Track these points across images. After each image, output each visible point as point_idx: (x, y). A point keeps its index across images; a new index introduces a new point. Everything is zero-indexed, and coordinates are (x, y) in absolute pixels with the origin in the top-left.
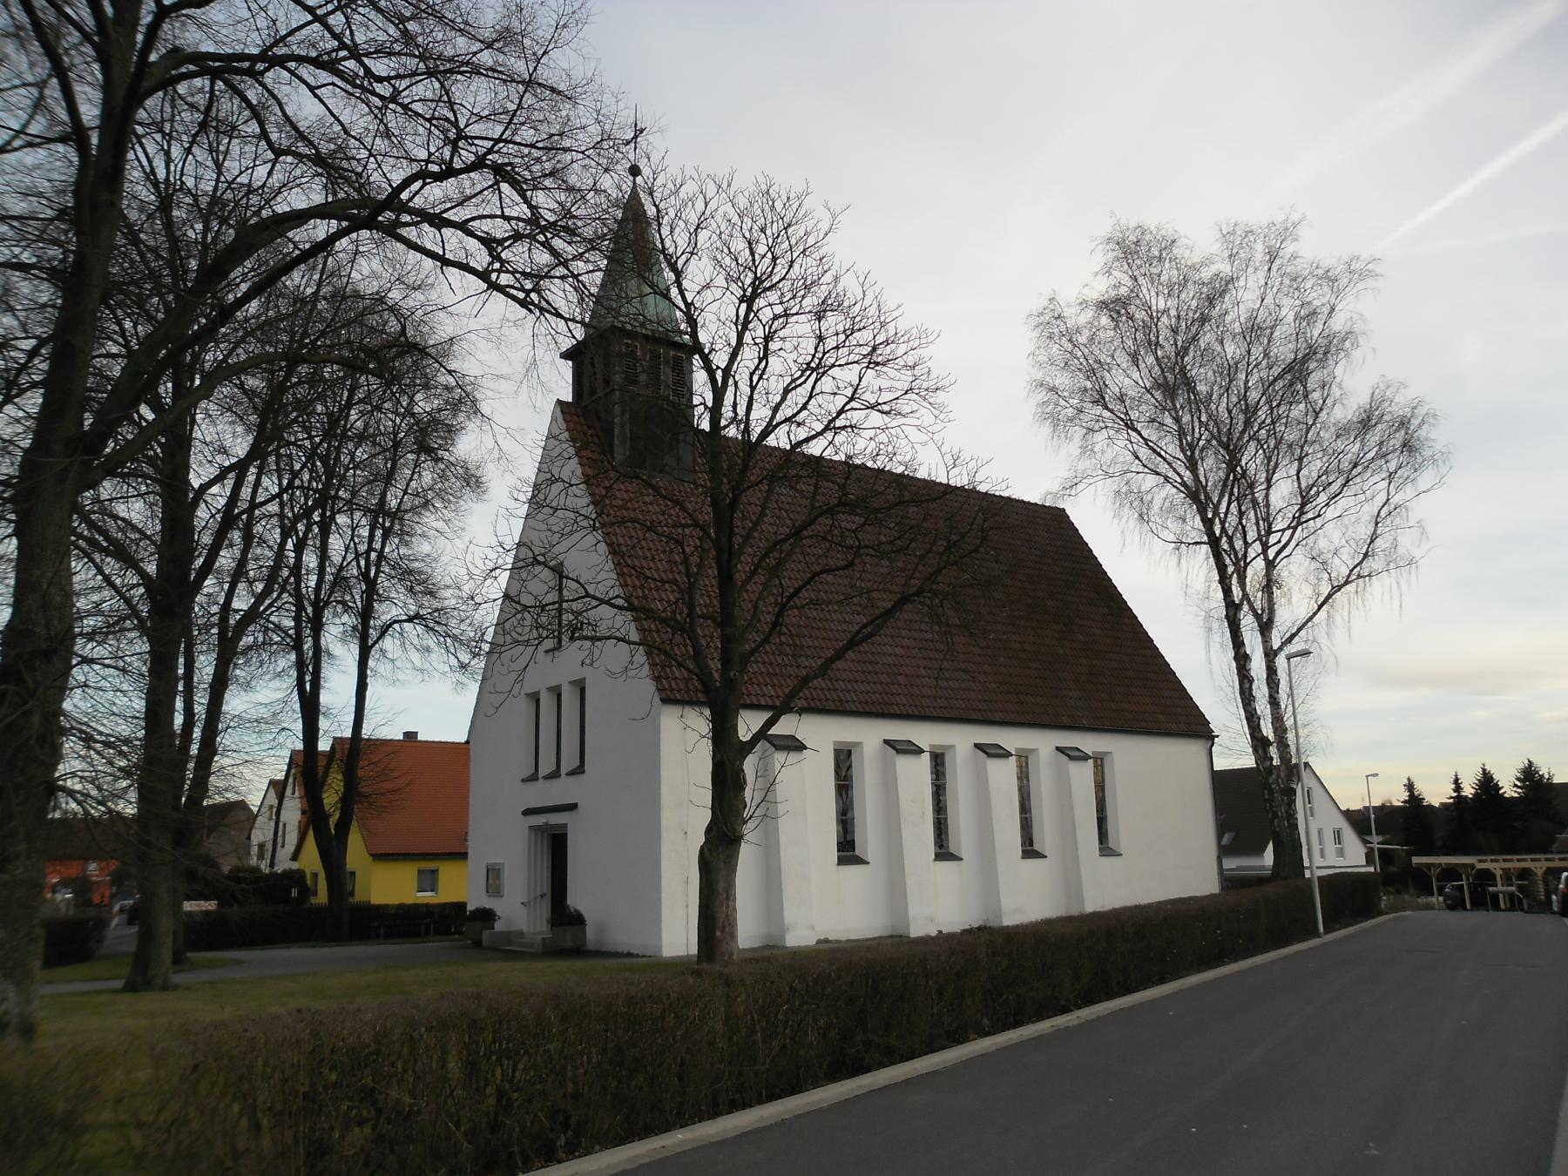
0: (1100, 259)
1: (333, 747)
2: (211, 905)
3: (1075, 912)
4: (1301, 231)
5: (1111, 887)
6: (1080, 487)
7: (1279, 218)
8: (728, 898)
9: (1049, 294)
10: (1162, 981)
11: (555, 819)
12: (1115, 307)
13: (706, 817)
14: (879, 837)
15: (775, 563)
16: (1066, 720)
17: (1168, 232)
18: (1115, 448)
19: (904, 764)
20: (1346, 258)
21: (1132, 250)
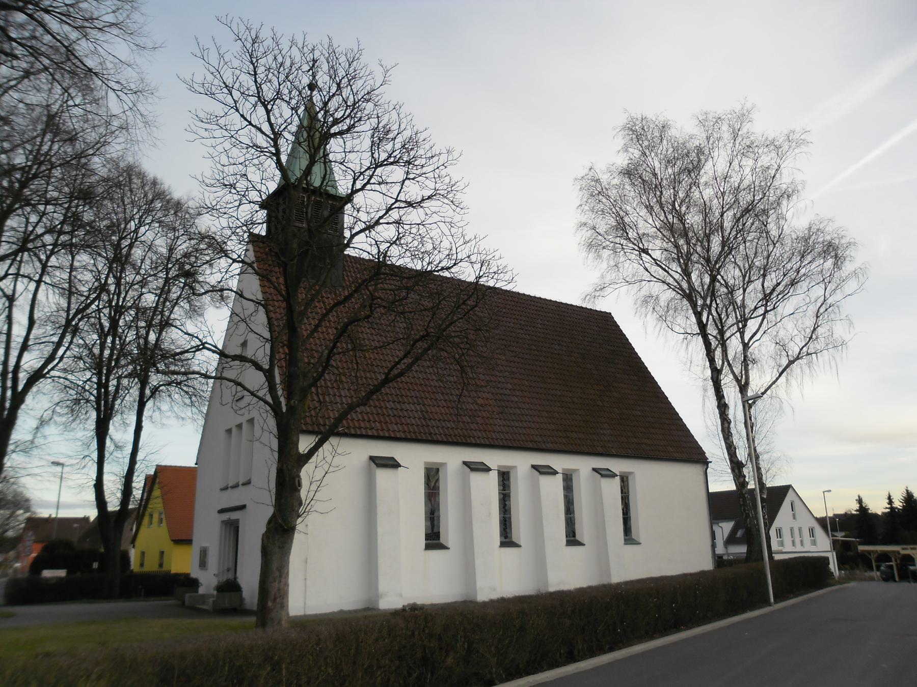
0: (620, 142)
1: (156, 472)
2: (62, 573)
3: (605, 582)
4: (754, 116)
5: (629, 566)
6: (608, 290)
7: (738, 108)
8: (280, 576)
9: (589, 165)
10: (611, 650)
11: (234, 515)
12: (628, 173)
13: (269, 511)
14: (390, 531)
15: (368, 335)
16: (600, 450)
17: (662, 119)
18: (631, 266)
19: (476, 479)
20: (785, 132)
21: (639, 133)
